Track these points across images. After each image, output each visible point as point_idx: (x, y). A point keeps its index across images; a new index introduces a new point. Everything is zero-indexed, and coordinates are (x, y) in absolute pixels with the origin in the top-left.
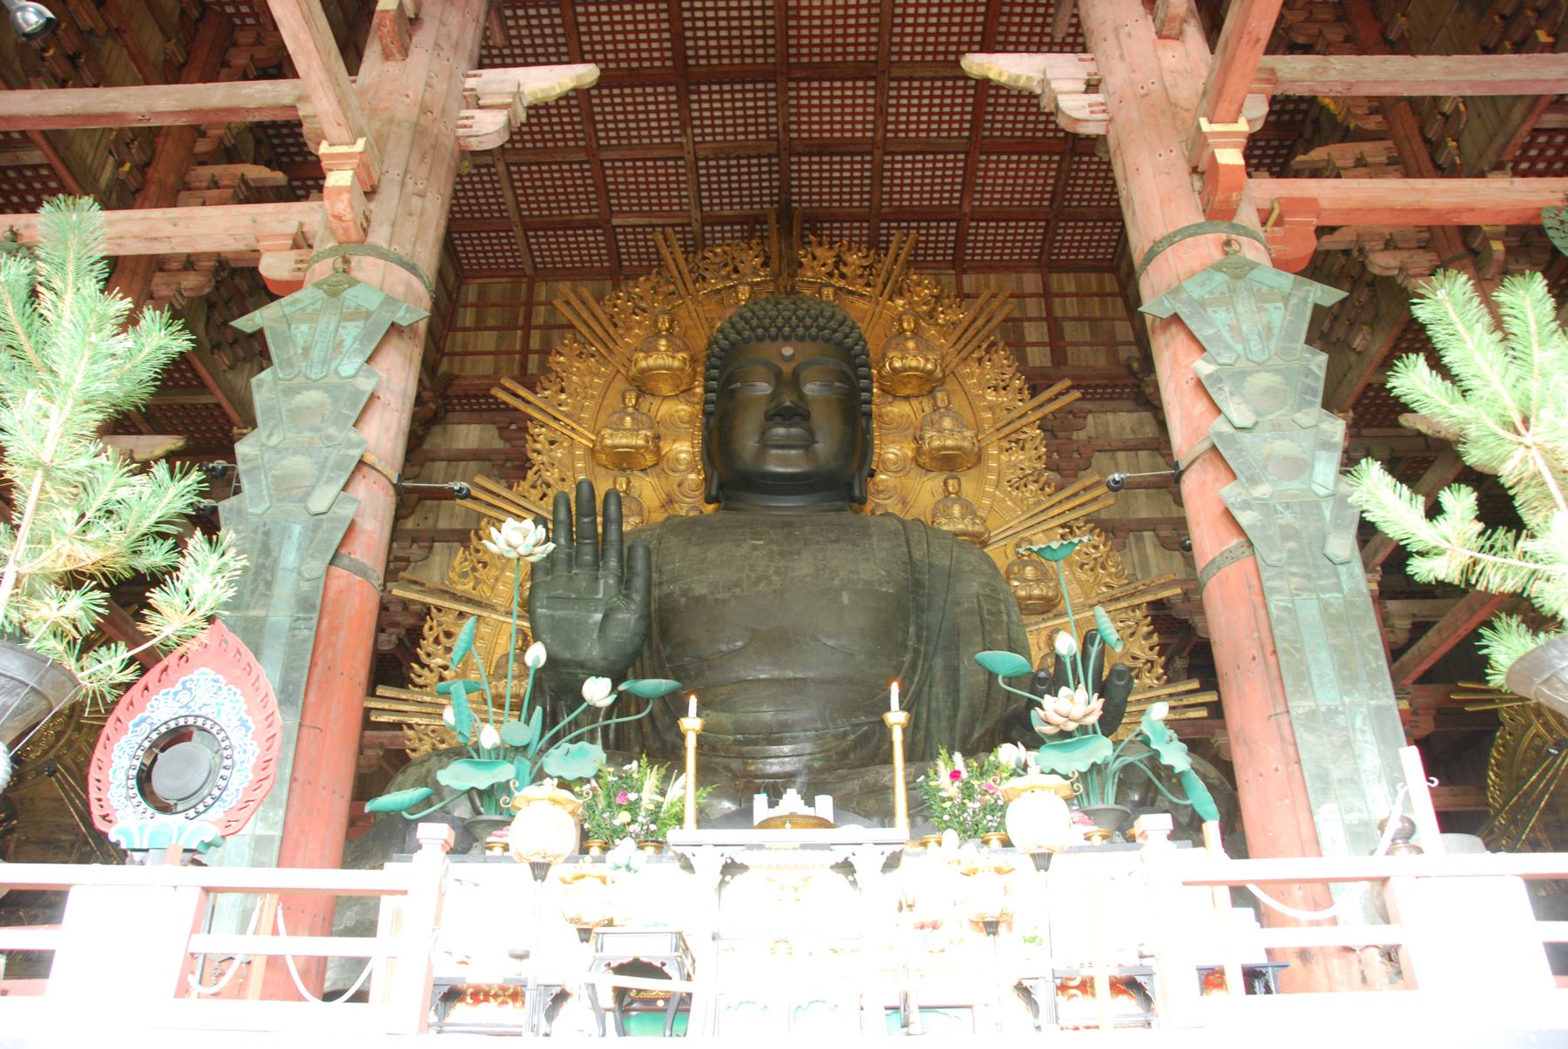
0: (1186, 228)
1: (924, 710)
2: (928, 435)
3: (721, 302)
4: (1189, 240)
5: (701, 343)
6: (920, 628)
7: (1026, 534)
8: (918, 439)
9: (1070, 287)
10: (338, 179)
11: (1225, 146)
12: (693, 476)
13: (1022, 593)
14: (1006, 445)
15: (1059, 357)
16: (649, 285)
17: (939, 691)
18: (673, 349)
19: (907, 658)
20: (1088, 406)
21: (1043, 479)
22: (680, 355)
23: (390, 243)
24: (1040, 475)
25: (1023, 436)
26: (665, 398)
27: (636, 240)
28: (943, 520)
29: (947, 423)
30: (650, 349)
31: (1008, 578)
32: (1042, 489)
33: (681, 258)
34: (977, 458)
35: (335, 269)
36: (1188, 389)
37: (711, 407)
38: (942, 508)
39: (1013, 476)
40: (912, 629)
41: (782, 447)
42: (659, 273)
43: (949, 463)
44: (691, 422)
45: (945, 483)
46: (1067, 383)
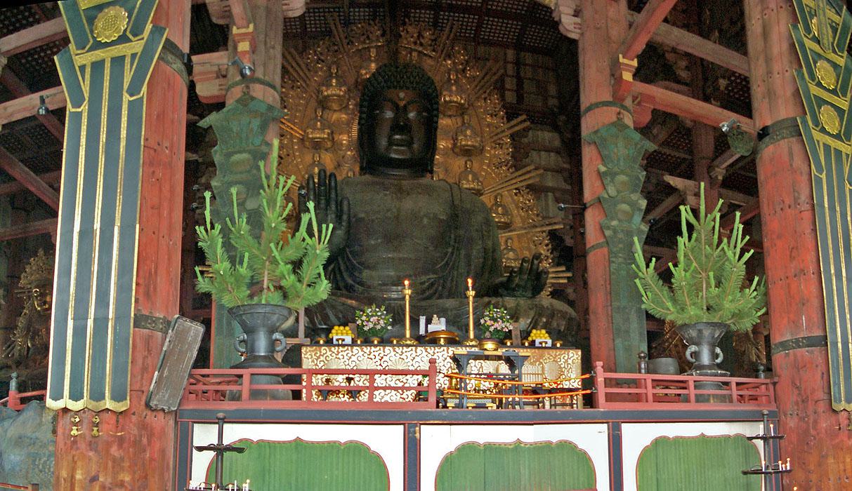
0: (604, 102)
1: (455, 273)
2: (460, 138)
3: (361, 57)
4: (605, 108)
5: (351, 80)
6: (456, 236)
7: (499, 191)
8: (455, 139)
9: (529, 61)
10: (244, 46)
11: (626, 70)
12: (349, 153)
13: (497, 220)
14: (494, 145)
15: (520, 98)
16: (324, 46)
17: (462, 264)
18: (339, 85)
19: (450, 250)
20: (532, 126)
21: (509, 165)
22: (343, 89)
23: (264, 76)
24: (508, 163)
25: (502, 142)
26: (335, 111)
27: (315, 16)
28: (464, 182)
29: (468, 132)
30: (329, 85)
31: (491, 213)
32: (508, 170)
33: (340, 30)
34: (482, 150)
35: (244, 93)
36: (595, 175)
37: (363, 122)
38: (464, 175)
39: (495, 161)
40: (453, 236)
41: (397, 145)
42: (329, 38)
43: (467, 152)
44: (349, 123)
45: (466, 163)
46: (524, 117)
